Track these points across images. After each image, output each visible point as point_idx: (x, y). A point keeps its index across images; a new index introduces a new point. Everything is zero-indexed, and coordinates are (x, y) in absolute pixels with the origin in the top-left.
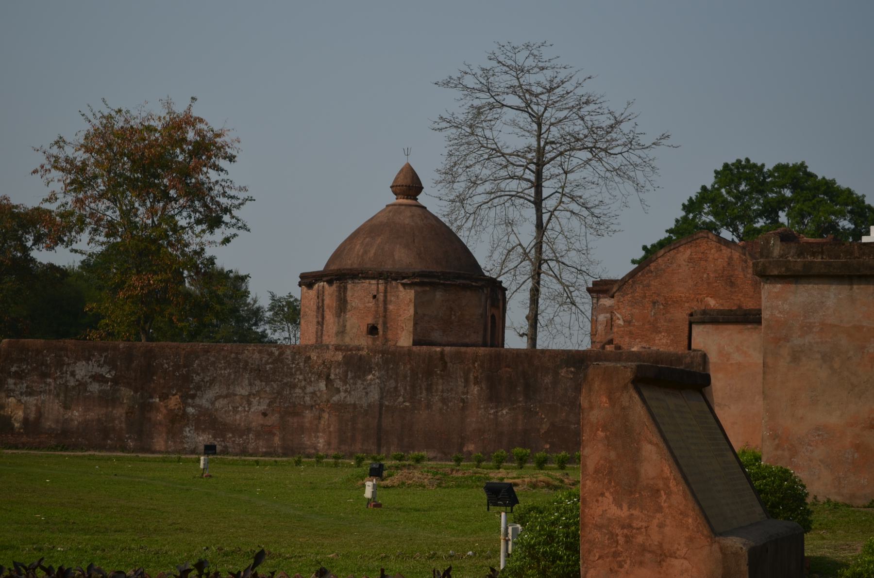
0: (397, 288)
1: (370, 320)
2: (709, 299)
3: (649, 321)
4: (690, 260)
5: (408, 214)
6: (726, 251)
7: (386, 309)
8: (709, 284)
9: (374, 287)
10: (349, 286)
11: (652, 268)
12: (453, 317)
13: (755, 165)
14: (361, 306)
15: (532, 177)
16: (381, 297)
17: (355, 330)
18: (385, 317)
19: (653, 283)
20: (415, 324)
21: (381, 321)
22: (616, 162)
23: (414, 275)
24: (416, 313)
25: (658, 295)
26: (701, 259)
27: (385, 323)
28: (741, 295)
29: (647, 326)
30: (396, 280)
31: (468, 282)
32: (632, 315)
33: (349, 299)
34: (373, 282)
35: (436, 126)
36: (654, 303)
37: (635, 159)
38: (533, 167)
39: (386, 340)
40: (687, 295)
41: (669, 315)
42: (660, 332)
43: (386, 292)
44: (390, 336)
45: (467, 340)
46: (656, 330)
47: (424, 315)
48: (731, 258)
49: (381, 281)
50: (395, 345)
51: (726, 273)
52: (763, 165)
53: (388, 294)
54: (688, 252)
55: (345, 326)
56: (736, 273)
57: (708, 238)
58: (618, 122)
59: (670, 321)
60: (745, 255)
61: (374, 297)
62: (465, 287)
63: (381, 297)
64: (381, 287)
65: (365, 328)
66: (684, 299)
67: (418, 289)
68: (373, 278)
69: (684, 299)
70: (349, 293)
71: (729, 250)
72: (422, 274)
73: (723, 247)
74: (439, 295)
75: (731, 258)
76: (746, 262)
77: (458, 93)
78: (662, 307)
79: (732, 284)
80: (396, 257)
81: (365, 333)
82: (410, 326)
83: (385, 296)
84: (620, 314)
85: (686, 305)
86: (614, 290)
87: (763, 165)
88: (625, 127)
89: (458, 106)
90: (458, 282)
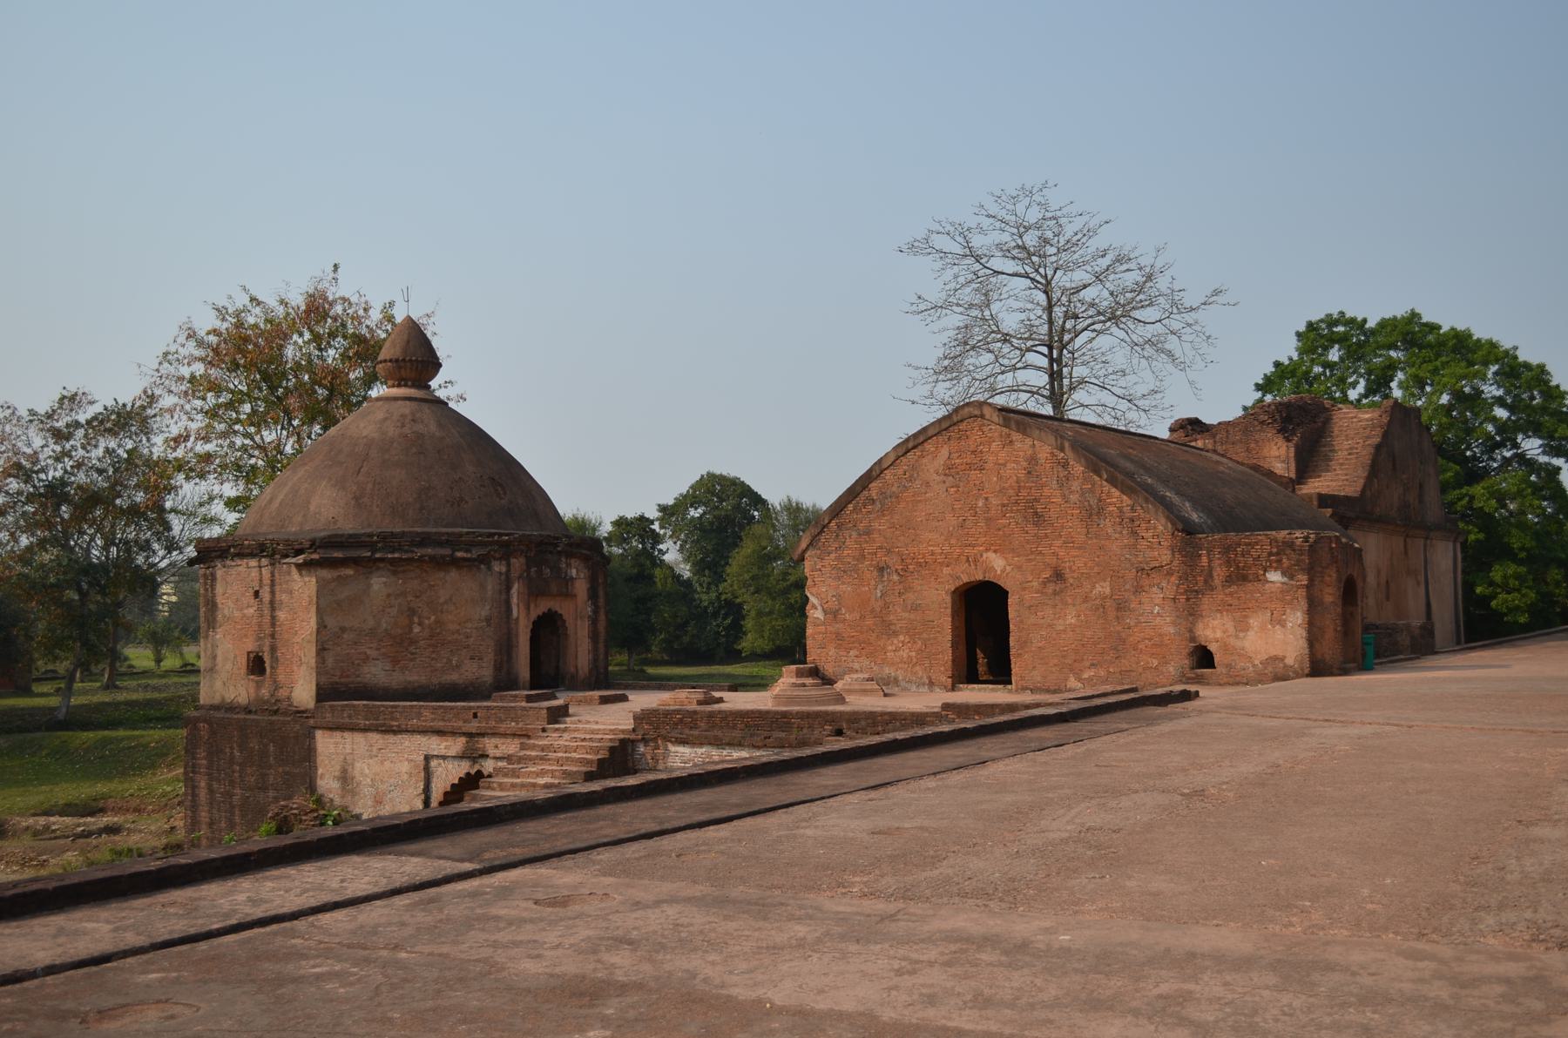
0: (289, 573)
1: (250, 645)
2: (991, 555)
3: (873, 611)
4: (949, 470)
5: (380, 415)
6: (1023, 444)
7: (273, 617)
8: (988, 520)
9: (254, 573)
10: (219, 573)
11: (874, 494)
12: (416, 629)
13: (1352, 321)
14: (237, 614)
15: (1044, 362)
16: (265, 595)
17: (229, 666)
18: (273, 636)
19: (876, 525)
20: (321, 650)
21: (266, 649)
22: (1149, 331)
23: (314, 545)
24: (322, 627)
25: (889, 551)
26: (970, 466)
27: (273, 649)
28: (1058, 543)
29: (869, 622)
30: (287, 556)
31: (447, 551)
32: (839, 597)
33: (219, 600)
34: (253, 563)
35: (914, 308)
36: (881, 570)
37: (1176, 326)
38: (1045, 350)
39: (277, 686)
40: (947, 548)
41: (911, 596)
42: (896, 634)
43: (273, 584)
44: (281, 678)
45: (454, 677)
46: (888, 630)
47: (343, 630)
48: (1033, 460)
49: (264, 561)
50: (289, 698)
51: (1024, 493)
52: (1365, 321)
53: (277, 588)
54: (945, 452)
55: (215, 657)
56: (1046, 492)
57: (982, 416)
58: (1149, 277)
59: (915, 608)
60: (1062, 449)
61: (256, 594)
62: (441, 564)
63: (265, 595)
64: (266, 572)
65: (243, 661)
66: (940, 559)
67: (326, 573)
68: (252, 555)
69: (940, 559)
70: (219, 589)
71: (1029, 441)
72: (334, 542)
73: (1016, 436)
74: (379, 584)
75: (1033, 460)
76: (1065, 465)
77: (928, 263)
78: (895, 578)
79: (1038, 519)
80: (312, 508)
81: (244, 670)
82: (309, 655)
83: (273, 593)
84: (817, 596)
85: (946, 571)
86: (804, 545)
87: (1365, 321)
88: (1162, 283)
89: (930, 279)
90: (419, 552)
